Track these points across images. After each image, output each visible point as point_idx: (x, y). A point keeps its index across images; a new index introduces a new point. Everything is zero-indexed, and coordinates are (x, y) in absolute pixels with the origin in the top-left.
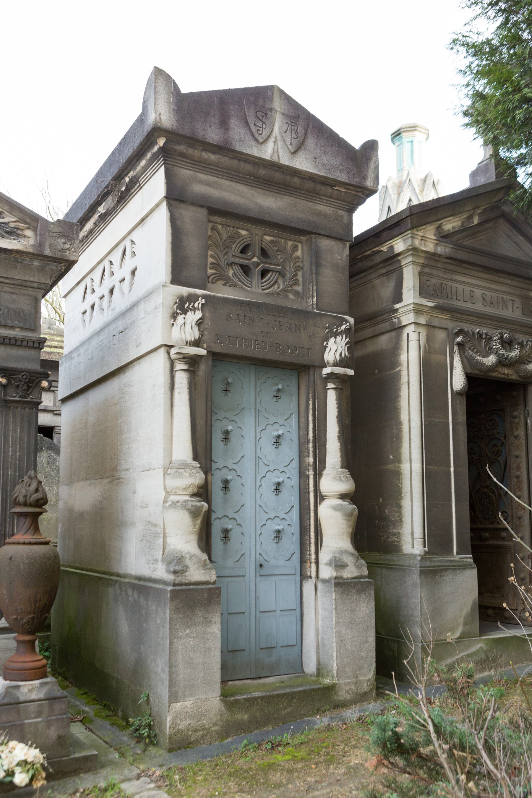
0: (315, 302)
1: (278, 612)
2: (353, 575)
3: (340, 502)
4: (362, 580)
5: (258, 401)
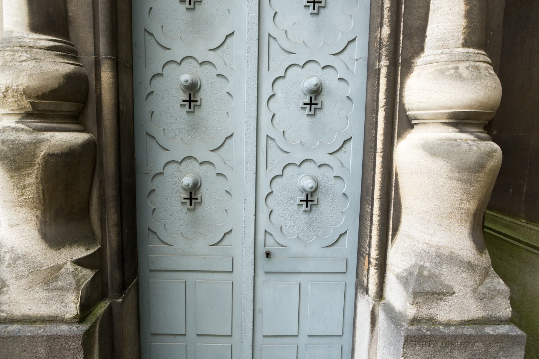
1: (303, 339)
2: (465, 317)
3: (451, 133)
4: (489, 330)
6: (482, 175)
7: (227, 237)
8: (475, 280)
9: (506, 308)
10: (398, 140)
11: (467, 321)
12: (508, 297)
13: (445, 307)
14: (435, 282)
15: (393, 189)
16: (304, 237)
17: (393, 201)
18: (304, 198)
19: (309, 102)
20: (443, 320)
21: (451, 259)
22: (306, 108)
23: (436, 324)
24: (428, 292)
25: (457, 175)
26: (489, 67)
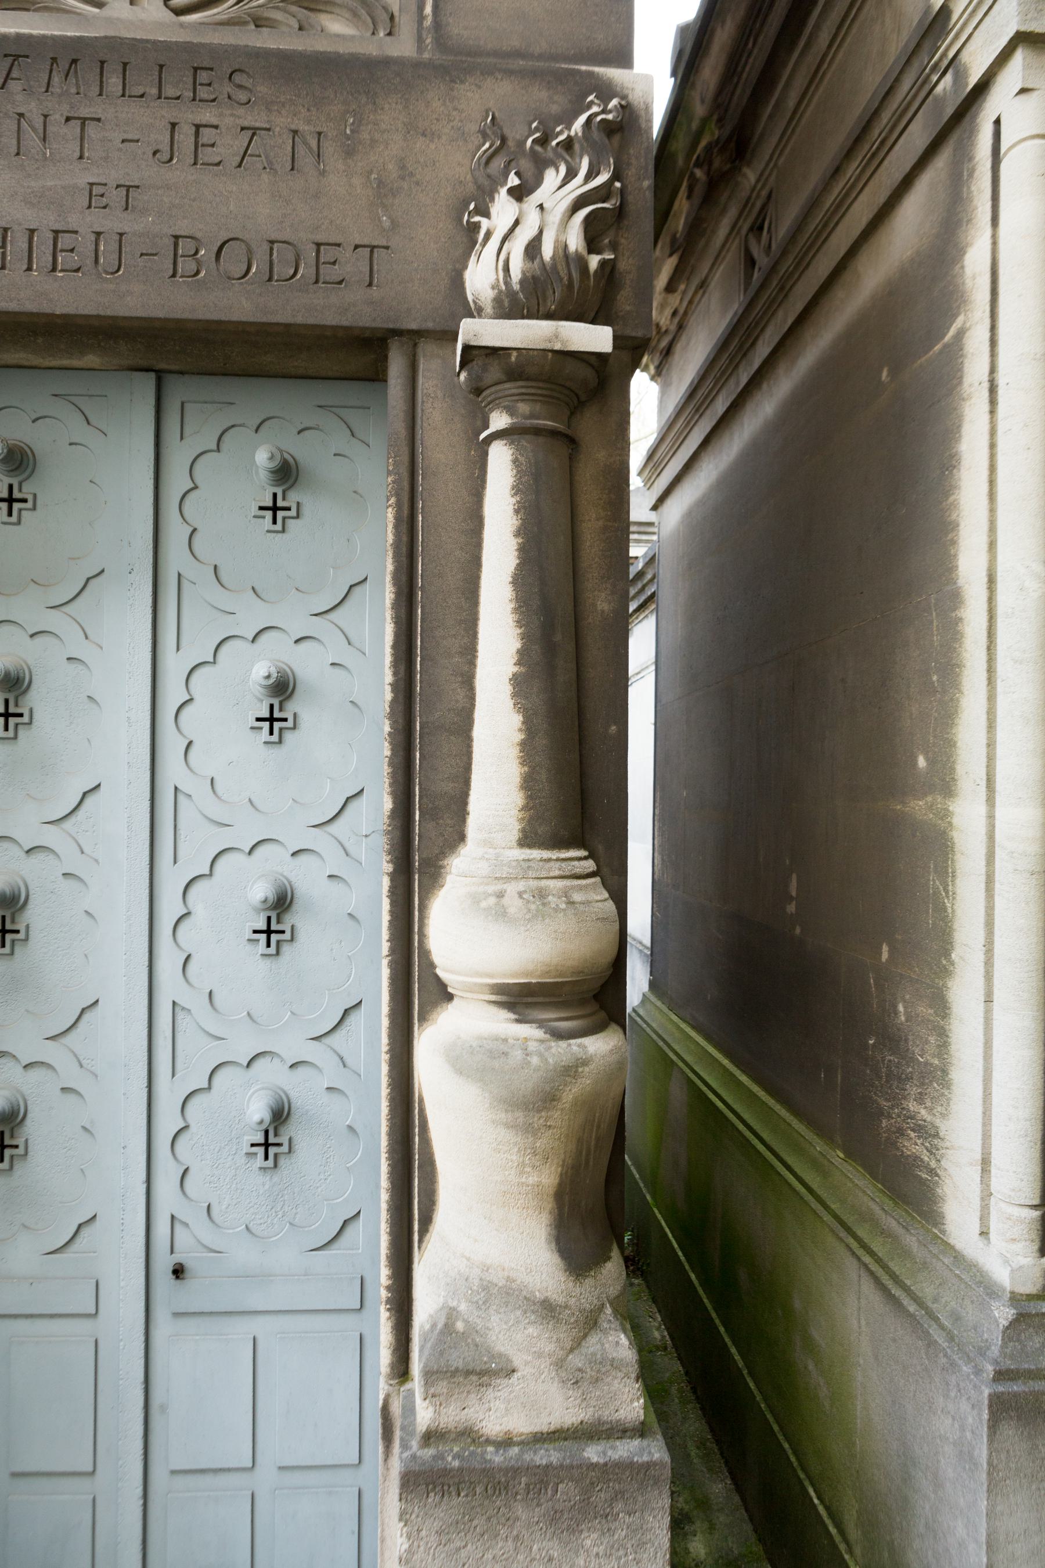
0: (428, 22)
1: (266, 1477)
2: (543, 1424)
3: (501, 1024)
4: (593, 1453)
5: (175, 532)
6: (557, 1114)
7: (85, 1232)
8: (558, 1340)
9: (632, 1401)
10: (420, 1026)
11: (548, 1434)
12: (633, 1376)
13: (498, 1402)
14: (477, 1346)
15: (417, 1130)
16: (263, 1227)
17: (417, 1157)
18: (260, 1138)
19: (265, 928)
20: (494, 1433)
21: (508, 1294)
22: (258, 940)
23: (479, 1443)
24: (457, 1370)
25: (503, 1115)
26: (573, 888)
